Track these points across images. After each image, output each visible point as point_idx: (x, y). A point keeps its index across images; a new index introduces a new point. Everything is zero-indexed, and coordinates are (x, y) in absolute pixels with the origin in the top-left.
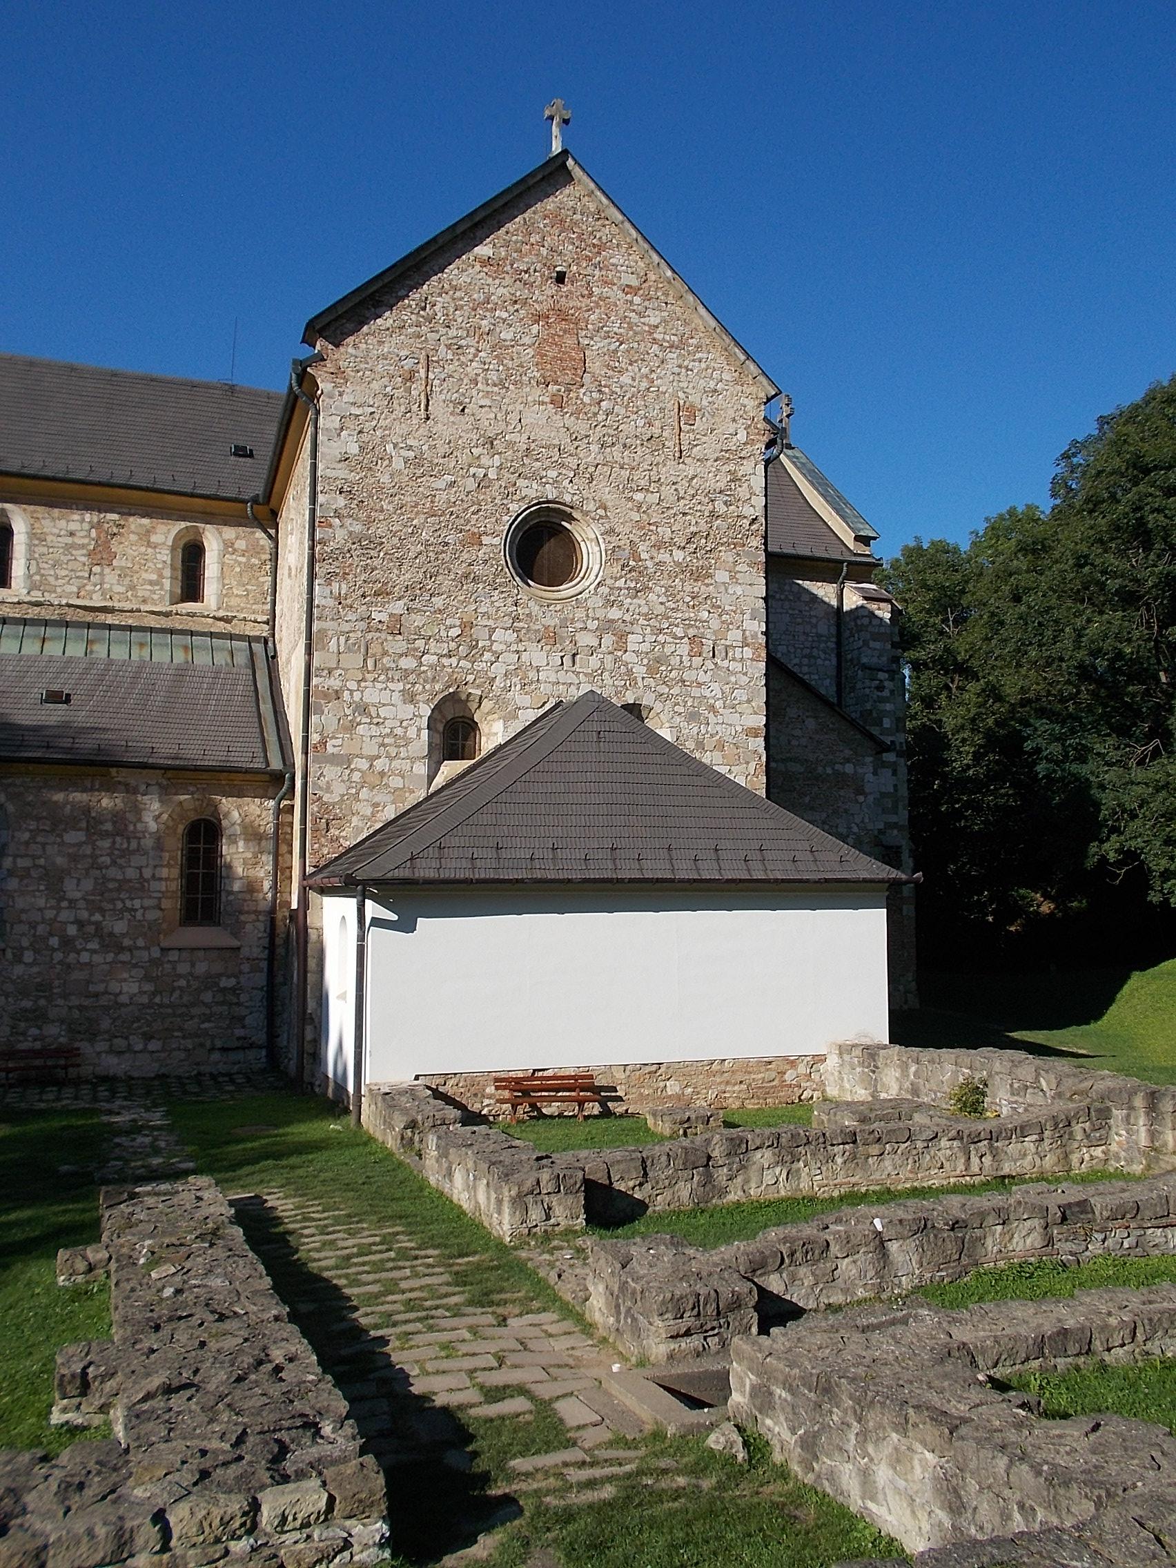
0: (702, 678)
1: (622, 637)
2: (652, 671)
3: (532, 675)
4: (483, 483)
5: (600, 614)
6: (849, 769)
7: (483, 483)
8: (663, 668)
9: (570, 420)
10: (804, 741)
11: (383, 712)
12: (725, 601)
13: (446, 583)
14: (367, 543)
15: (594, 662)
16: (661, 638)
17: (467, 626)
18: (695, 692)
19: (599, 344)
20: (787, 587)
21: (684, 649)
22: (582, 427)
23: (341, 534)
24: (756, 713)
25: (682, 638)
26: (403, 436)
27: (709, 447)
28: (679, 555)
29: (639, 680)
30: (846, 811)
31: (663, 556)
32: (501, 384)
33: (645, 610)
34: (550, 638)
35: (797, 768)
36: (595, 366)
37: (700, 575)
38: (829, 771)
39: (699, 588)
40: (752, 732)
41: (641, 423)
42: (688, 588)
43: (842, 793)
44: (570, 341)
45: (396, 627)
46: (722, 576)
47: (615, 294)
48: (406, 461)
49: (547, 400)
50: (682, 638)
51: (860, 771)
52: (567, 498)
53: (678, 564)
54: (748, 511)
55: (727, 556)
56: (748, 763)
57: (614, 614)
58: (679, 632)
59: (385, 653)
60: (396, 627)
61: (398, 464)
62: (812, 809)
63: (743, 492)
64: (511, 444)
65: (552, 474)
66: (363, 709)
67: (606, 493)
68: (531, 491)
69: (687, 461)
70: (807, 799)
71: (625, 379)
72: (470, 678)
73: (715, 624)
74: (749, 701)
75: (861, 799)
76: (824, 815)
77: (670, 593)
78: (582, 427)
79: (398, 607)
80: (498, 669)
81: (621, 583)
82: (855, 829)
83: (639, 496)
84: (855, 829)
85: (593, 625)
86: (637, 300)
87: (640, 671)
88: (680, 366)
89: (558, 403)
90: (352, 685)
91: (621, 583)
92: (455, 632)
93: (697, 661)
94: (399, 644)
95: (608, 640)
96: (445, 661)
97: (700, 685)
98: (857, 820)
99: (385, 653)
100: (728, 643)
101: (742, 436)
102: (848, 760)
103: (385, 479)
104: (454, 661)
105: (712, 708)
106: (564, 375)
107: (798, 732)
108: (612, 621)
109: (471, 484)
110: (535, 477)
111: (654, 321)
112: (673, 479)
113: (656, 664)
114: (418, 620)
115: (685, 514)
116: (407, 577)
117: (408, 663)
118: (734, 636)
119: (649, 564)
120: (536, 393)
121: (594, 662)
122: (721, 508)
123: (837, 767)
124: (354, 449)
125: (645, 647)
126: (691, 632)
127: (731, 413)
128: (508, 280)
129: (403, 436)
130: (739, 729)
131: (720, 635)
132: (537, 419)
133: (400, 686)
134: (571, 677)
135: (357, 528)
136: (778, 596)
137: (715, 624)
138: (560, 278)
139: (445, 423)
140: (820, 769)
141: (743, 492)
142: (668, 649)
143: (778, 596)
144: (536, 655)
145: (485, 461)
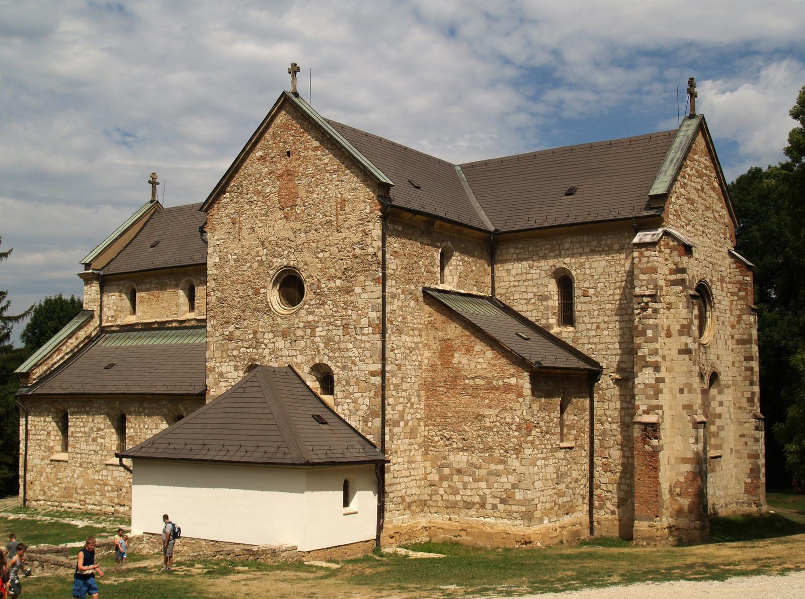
0: (350, 346)
1: (313, 329)
2: (326, 345)
3: (279, 353)
4: (261, 263)
5: (305, 319)
6: (513, 381)
7: (261, 263)
8: (331, 343)
9: (292, 224)
10: (485, 366)
11: (229, 375)
12: (360, 303)
13: (248, 313)
14: (222, 300)
15: (302, 343)
16: (331, 328)
17: (255, 333)
18: (346, 354)
19: (304, 181)
20: (603, 242)
21: (340, 333)
22: (297, 225)
23: (214, 298)
24: (374, 363)
25: (339, 326)
26: (235, 248)
27: (353, 220)
28: (338, 282)
29: (321, 350)
30: (511, 408)
31: (332, 284)
32: (266, 215)
33: (323, 314)
34: (284, 335)
35: (480, 382)
36: (302, 193)
37: (348, 291)
38: (501, 383)
39: (348, 298)
40: (373, 374)
41: (321, 216)
42: (342, 299)
43: (508, 396)
44: (291, 184)
45: (230, 338)
46: (358, 290)
47: (311, 152)
48: (235, 260)
49: (283, 216)
50: (339, 326)
51: (521, 382)
52: (292, 263)
53: (338, 287)
54: (371, 250)
55: (362, 278)
56: (370, 391)
57: (310, 318)
58: (339, 323)
59: (228, 349)
60: (230, 338)
61: (232, 263)
62: (490, 407)
63: (369, 240)
64: (270, 242)
65: (286, 253)
66: (221, 375)
67: (307, 256)
68: (278, 262)
69: (342, 230)
70: (487, 401)
71: (315, 196)
72: (257, 357)
73: (355, 317)
74: (371, 357)
75: (521, 400)
76: (498, 410)
77: (335, 304)
78: (297, 225)
79: (231, 328)
80: (267, 351)
81: (313, 302)
82: (517, 420)
83: (321, 255)
84: (517, 420)
85: (301, 325)
86: (319, 153)
87: (322, 345)
88: (338, 181)
89: (286, 217)
90: (218, 365)
91: (313, 302)
92: (251, 337)
93: (347, 337)
94: (232, 345)
95: (309, 331)
96: (248, 350)
97: (347, 350)
98: (518, 413)
99: (228, 349)
100: (361, 326)
101: (368, 210)
102: (513, 376)
103: (228, 270)
104: (251, 349)
105: (354, 363)
106: (288, 203)
107: (481, 360)
108: (309, 322)
109: (256, 265)
110: (281, 256)
111: (326, 161)
112: (336, 242)
113: (328, 341)
114: (238, 333)
115: (342, 260)
116: (236, 313)
117: (235, 353)
118: (364, 321)
119: (325, 290)
120: (280, 214)
121: (302, 343)
122: (358, 251)
123: (505, 380)
124: (217, 260)
125: (324, 333)
126: (345, 322)
127: (362, 198)
128: (268, 164)
129: (235, 248)
130: (367, 372)
131: (357, 322)
132: (280, 228)
133: (232, 363)
134: (294, 353)
135: (219, 295)
136: (597, 249)
137: (355, 317)
138: (289, 154)
139: (249, 240)
140: (495, 382)
141: (369, 240)
142: (335, 332)
143: (597, 249)
144: (280, 343)
145: (260, 253)
